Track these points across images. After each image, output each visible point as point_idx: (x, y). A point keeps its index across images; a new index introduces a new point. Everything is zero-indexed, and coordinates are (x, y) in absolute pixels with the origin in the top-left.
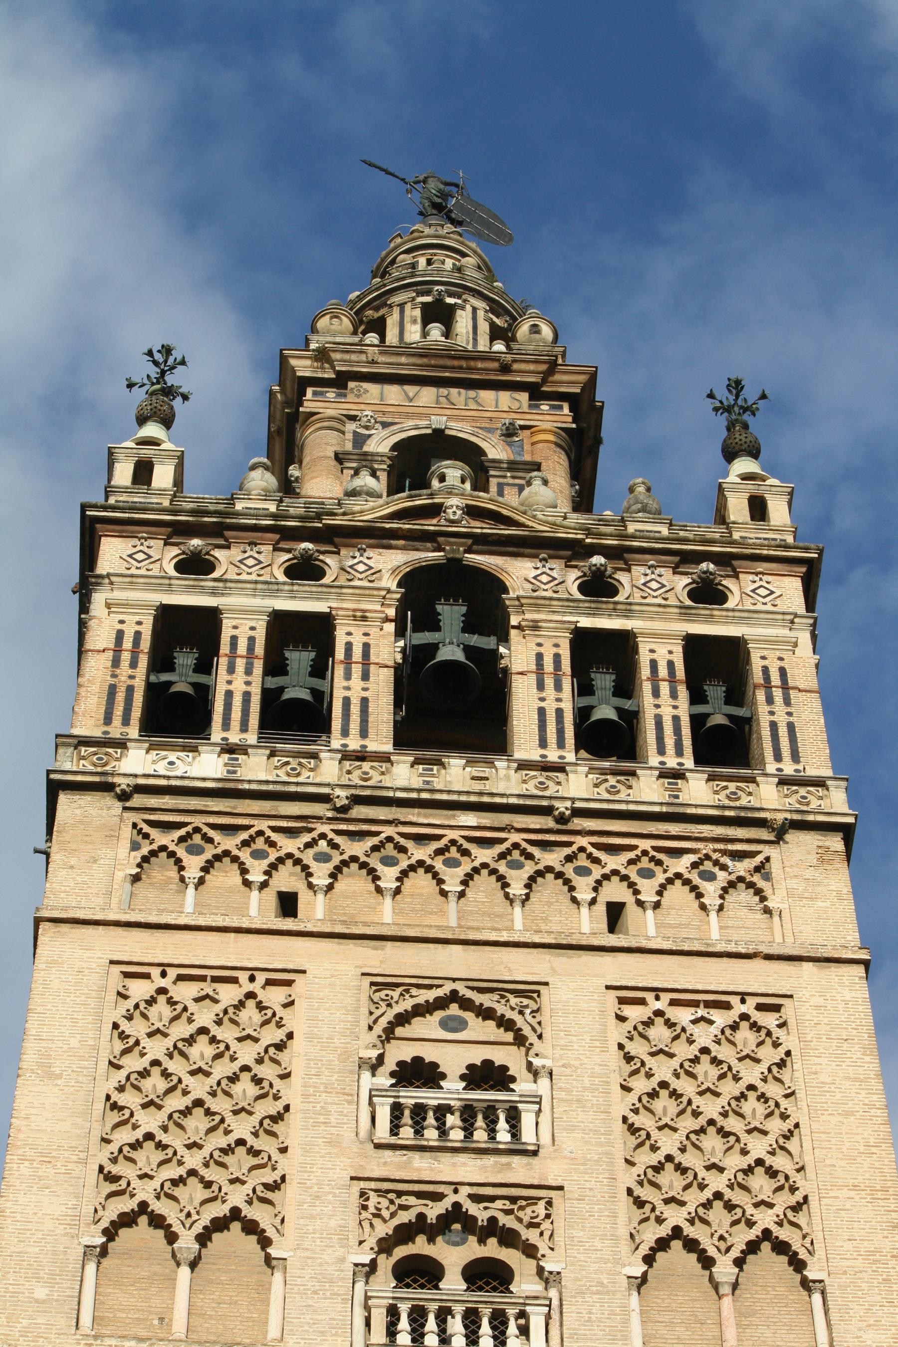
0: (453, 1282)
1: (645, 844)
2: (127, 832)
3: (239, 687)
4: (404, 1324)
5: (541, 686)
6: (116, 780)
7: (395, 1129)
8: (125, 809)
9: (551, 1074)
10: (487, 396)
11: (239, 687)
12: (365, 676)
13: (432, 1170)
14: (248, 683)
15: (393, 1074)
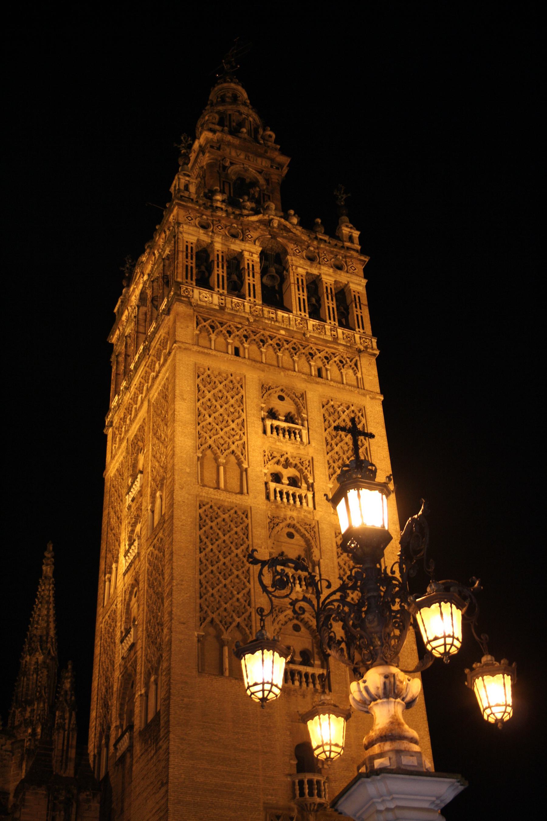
0: (285, 481)
1: (327, 349)
2: (195, 317)
3: (220, 273)
4: (278, 495)
5: (299, 290)
6: (193, 300)
7: (272, 433)
8: (194, 311)
9: (307, 421)
10: (259, 160)
11: (220, 273)
12: (253, 277)
13: (281, 446)
14: (223, 272)
15: (268, 412)
